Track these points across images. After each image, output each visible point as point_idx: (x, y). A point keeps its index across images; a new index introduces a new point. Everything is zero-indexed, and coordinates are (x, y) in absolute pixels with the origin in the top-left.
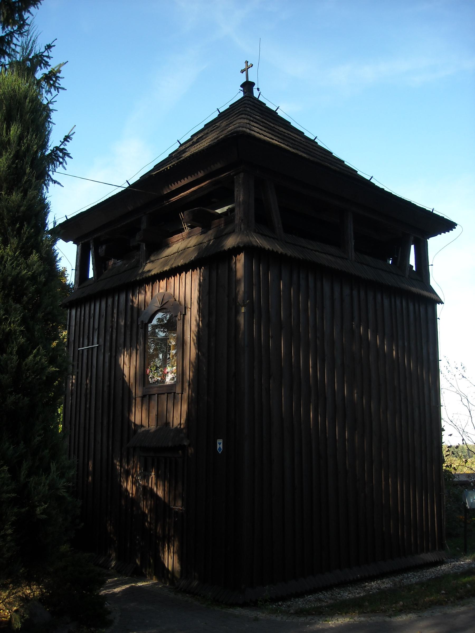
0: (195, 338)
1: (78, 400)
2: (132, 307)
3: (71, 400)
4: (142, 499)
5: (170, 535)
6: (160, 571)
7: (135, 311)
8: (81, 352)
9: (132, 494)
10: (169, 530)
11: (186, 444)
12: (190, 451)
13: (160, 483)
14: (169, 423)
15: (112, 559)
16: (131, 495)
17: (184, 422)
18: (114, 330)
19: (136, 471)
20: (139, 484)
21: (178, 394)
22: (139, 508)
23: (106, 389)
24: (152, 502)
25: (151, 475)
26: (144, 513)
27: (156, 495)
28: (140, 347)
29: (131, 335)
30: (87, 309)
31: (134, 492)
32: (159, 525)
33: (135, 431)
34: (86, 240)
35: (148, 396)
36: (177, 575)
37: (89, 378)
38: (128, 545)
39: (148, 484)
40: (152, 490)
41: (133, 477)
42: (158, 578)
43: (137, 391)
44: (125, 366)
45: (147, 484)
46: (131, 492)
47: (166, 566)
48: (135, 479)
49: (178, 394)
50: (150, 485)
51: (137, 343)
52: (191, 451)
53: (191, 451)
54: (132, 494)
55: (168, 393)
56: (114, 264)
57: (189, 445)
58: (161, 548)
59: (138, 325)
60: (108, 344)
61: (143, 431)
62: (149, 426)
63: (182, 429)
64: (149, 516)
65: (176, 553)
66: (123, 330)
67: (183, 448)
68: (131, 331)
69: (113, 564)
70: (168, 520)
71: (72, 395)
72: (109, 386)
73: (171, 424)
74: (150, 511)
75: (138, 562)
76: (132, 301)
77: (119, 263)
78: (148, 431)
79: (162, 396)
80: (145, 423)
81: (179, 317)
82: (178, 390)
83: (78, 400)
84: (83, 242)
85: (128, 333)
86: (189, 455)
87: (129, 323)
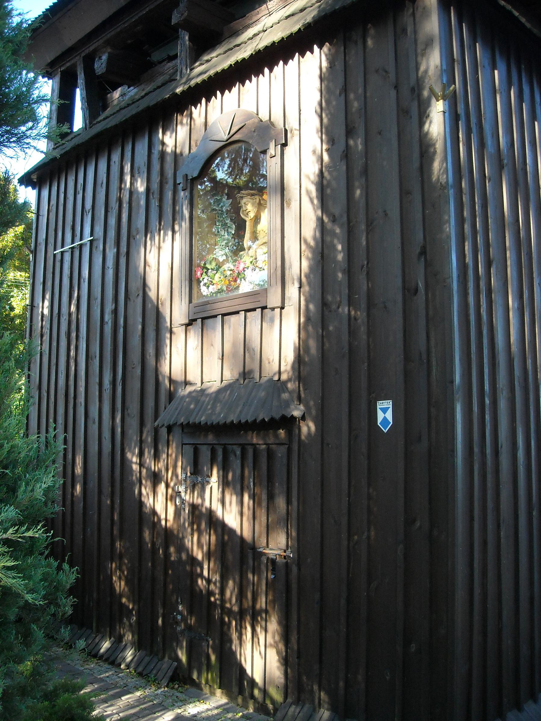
0: (313, 189)
1: (54, 344)
2: (163, 155)
3: (41, 344)
4: (189, 530)
5: (258, 606)
6: (234, 679)
7: (169, 160)
8: (59, 257)
9: (166, 520)
10: (255, 599)
11: (297, 413)
12: (304, 430)
13: (231, 499)
14: (251, 372)
15: (126, 645)
16: (163, 523)
17: (289, 368)
18: (125, 206)
19: (175, 474)
20: (183, 501)
21: (273, 309)
22: (181, 548)
23: (108, 317)
24: (213, 538)
25: (208, 482)
26: (193, 560)
27: (223, 525)
28: (180, 226)
29: (161, 207)
30: (71, 184)
31: (171, 516)
32: (231, 583)
33: (171, 396)
34: (68, 64)
35: (199, 321)
36: (277, 696)
37: (74, 302)
38: (160, 622)
39: (203, 499)
40: (211, 513)
41: (167, 486)
42: (228, 693)
43: (177, 312)
44: (147, 268)
45: (200, 501)
46: (163, 516)
47: (249, 672)
48: (173, 489)
49: (273, 309)
50: (207, 504)
51: (174, 220)
52: (308, 428)
53: (308, 428)
54: (166, 520)
55: (247, 311)
56: (123, 95)
57: (303, 418)
58: (235, 636)
59: (175, 185)
60: (112, 233)
61: (190, 393)
62: (202, 383)
63: (285, 383)
64: (206, 566)
65: (271, 645)
66: (143, 202)
67: (289, 423)
68: (161, 200)
69: (129, 655)
70: (250, 576)
71: (42, 336)
72: (115, 312)
73: (257, 375)
74: (209, 555)
75: (183, 656)
76: (163, 144)
77: (133, 92)
78: (203, 391)
79: (233, 319)
80: (193, 376)
81: (271, 151)
82: (274, 300)
83: (54, 344)
84: (62, 69)
85: (155, 204)
86: (303, 437)
87: (155, 186)
